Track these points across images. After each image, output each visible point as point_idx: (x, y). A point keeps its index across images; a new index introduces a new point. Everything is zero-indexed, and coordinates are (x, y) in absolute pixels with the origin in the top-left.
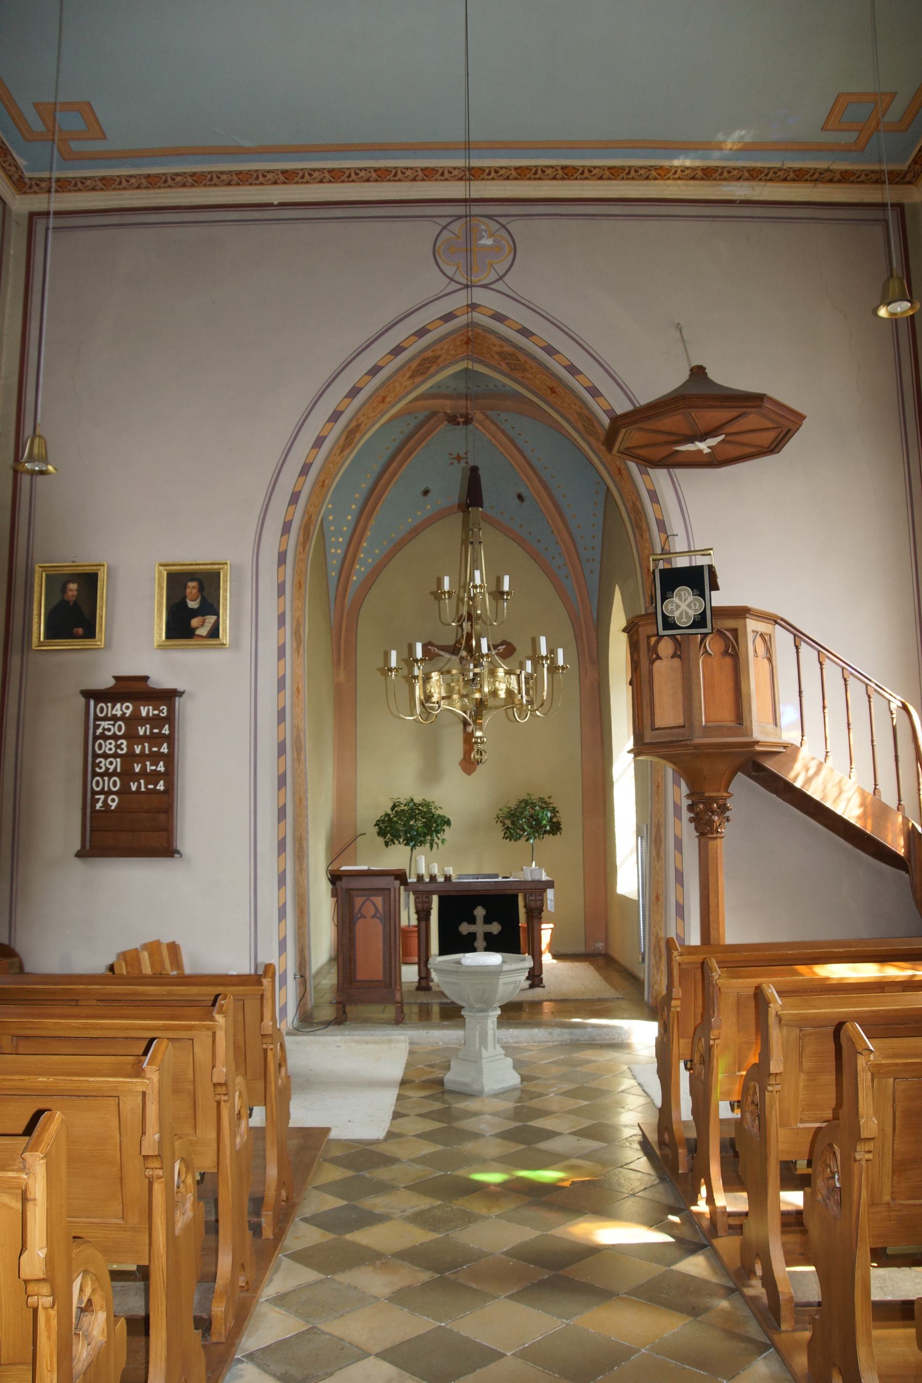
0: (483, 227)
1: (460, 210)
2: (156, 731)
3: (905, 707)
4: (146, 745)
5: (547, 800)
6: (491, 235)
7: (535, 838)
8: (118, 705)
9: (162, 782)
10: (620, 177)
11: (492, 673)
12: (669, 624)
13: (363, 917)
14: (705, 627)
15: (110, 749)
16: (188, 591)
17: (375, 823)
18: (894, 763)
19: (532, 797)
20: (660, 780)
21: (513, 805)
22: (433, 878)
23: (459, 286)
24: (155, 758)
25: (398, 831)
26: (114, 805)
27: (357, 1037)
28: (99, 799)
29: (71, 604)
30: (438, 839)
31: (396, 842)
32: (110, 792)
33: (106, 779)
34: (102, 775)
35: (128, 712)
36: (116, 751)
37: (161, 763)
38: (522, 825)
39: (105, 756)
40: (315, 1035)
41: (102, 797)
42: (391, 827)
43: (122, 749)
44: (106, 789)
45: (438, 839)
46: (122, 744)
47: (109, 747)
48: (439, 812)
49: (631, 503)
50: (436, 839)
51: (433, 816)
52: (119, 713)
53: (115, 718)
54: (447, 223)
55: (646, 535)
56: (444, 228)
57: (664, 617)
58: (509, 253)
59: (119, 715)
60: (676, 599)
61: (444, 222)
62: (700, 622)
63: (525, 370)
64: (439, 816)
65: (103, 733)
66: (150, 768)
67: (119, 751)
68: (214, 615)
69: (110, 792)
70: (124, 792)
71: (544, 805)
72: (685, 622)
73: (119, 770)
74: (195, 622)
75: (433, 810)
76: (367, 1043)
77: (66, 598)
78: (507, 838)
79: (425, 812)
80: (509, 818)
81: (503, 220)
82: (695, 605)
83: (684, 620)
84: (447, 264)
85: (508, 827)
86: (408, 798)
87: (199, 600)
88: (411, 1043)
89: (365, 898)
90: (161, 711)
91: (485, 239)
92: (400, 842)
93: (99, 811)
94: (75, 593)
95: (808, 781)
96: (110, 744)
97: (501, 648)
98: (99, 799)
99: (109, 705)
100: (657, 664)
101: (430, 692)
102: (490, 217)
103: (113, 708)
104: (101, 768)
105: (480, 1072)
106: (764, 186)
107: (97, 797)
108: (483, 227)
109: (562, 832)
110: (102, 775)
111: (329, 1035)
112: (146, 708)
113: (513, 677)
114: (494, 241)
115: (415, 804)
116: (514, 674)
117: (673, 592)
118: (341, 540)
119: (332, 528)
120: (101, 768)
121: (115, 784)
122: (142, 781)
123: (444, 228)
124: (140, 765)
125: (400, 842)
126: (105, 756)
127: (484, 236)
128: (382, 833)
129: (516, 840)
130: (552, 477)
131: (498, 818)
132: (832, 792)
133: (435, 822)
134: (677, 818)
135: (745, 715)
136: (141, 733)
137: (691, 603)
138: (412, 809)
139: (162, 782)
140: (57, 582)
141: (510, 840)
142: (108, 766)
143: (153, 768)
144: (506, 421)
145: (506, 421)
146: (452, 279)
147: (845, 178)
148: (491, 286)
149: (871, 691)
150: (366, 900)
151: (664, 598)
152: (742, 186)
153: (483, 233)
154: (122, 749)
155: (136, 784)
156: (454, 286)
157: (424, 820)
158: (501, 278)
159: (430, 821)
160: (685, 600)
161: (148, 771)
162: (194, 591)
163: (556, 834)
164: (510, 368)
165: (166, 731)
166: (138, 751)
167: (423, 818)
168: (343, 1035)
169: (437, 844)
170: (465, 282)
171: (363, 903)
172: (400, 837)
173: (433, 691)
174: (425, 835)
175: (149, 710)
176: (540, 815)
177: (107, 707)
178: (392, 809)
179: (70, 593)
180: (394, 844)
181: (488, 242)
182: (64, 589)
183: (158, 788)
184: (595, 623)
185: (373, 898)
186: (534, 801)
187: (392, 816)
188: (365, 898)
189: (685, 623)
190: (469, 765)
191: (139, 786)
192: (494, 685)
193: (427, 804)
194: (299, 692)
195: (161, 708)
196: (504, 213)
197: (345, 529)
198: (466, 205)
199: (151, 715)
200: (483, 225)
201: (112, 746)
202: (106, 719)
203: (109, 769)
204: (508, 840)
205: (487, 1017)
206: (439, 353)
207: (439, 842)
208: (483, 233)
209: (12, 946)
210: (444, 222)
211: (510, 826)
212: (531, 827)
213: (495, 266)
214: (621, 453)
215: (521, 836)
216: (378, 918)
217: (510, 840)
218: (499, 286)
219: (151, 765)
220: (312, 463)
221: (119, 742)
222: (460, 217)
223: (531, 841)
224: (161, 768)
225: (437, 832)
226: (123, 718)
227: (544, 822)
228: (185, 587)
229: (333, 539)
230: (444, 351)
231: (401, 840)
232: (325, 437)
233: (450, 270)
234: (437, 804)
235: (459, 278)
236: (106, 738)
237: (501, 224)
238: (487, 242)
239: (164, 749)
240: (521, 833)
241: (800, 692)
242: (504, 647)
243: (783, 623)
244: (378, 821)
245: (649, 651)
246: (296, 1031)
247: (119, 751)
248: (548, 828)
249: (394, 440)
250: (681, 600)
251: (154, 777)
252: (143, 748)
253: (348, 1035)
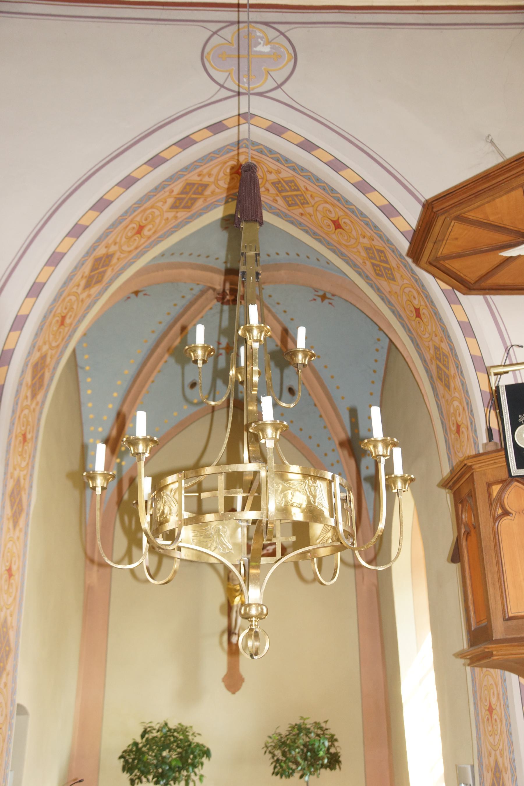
0: (258, 34)
1: (231, 15)
5: (323, 725)
6: (268, 42)
7: (311, 774)
11: (282, 475)
17: (120, 754)
19: (306, 722)
20: (494, 701)
21: (284, 731)
23: (230, 94)
25: (146, 764)
30: (196, 774)
31: (144, 779)
38: (295, 758)
42: (139, 760)
45: (196, 774)
48: (197, 740)
49: (432, 351)
50: (193, 774)
51: (190, 745)
55: (456, 383)
56: (215, 33)
58: (289, 61)
61: (215, 27)
63: (305, 203)
64: (198, 745)
71: (319, 732)
75: (190, 738)
78: (277, 774)
79: (181, 740)
80: (280, 747)
85: (278, 760)
86: (162, 722)
92: (148, 780)
100: (505, 521)
101: (163, 513)
102: (266, 24)
108: (258, 34)
109: (342, 766)
113: (321, 485)
114: (271, 48)
115: (170, 730)
116: (323, 479)
118: (100, 429)
119: (91, 416)
123: (215, 33)
125: (148, 780)
127: (260, 43)
128: (128, 768)
129: (289, 776)
130: (326, 367)
131: (267, 747)
133: (193, 753)
138: (166, 736)
141: (281, 777)
144: (278, 304)
145: (278, 304)
148: (268, 95)
153: (259, 40)
156: (225, 93)
157: (179, 750)
158: (279, 86)
159: (186, 751)
163: (335, 769)
164: (287, 202)
167: (178, 746)
169: (194, 781)
170: (236, 88)
172: (149, 773)
173: (167, 510)
174: (180, 770)
176: (317, 744)
178: (143, 736)
180: (141, 782)
186: (308, 726)
187: (140, 745)
192: (285, 496)
193: (183, 730)
194: (10, 575)
196: (284, 20)
197: (105, 418)
198: (239, 11)
200: (259, 32)
204: (279, 776)
206: (206, 180)
207: (196, 779)
208: (259, 40)
210: (215, 27)
211: (281, 758)
212: (305, 759)
214: (430, 263)
215: (294, 771)
217: (281, 777)
218: (277, 94)
220: (45, 284)
222: (232, 23)
223: (306, 778)
225: (194, 766)
227: (321, 754)
229: (92, 428)
230: (212, 179)
231: (150, 777)
232: (63, 255)
233: (220, 77)
234: (195, 729)
240: (294, 767)
244: (125, 751)
248: (326, 761)
249: (160, 323)
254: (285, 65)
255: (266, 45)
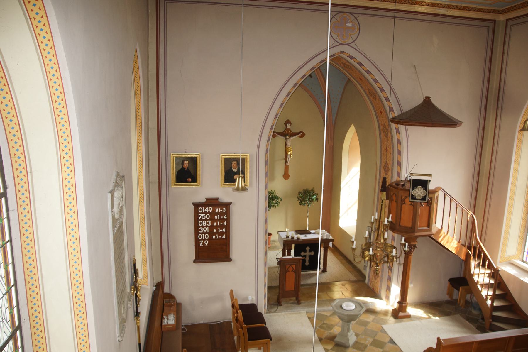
0: (348, 18)
2: (222, 217)
3: (472, 216)
4: (218, 222)
6: (351, 22)
8: (207, 208)
9: (224, 235)
10: (402, 3)
12: (413, 197)
13: (289, 271)
14: (425, 200)
15: (204, 224)
16: (233, 165)
18: (444, 200)
21: (301, 191)
22: (293, 238)
24: (222, 227)
26: (207, 244)
27: (290, 312)
28: (201, 242)
29: (186, 169)
32: (205, 239)
33: (203, 235)
34: (202, 233)
35: (211, 211)
36: (207, 225)
37: (224, 229)
39: (203, 227)
40: (276, 313)
41: (202, 241)
43: (209, 224)
44: (204, 238)
46: (209, 222)
47: (204, 223)
48: (276, 194)
52: (207, 211)
53: (206, 213)
54: (335, 14)
57: (412, 195)
58: (357, 31)
59: (207, 212)
60: (417, 190)
62: (424, 198)
65: (202, 218)
66: (220, 230)
67: (208, 225)
68: (243, 174)
69: (205, 239)
70: (210, 239)
72: (419, 198)
73: (208, 232)
74: (235, 177)
76: (293, 314)
77: (184, 167)
81: (356, 15)
82: (423, 193)
83: (419, 197)
84: (334, 34)
87: (237, 168)
88: (307, 312)
89: (289, 266)
90: (224, 210)
91: (348, 23)
93: (201, 246)
94: (188, 165)
95: (442, 240)
96: (205, 222)
97: (300, 134)
98: (201, 242)
99: (203, 208)
100: (404, 205)
102: (351, 13)
103: (205, 210)
104: (201, 231)
105: (348, 340)
106: (451, 10)
107: (200, 241)
110: (202, 233)
111: (280, 312)
112: (218, 209)
117: (416, 187)
120: (201, 231)
121: (207, 236)
122: (217, 235)
124: (216, 230)
126: (203, 227)
132: (447, 242)
134: (393, 240)
135: (430, 225)
136: (216, 218)
137: (422, 192)
139: (224, 235)
140: (180, 160)
142: (204, 230)
143: (221, 230)
146: (335, 41)
147: (480, 10)
149: (464, 211)
150: (289, 266)
151: (413, 189)
152: (444, 10)
154: (209, 224)
155: (215, 236)
158: (354, 42)
160: (420, 191)
161: (219, 231)
162: (235, 165)
165: (225, 217)
166: (215, 225)
168: (285, 312)
171: (288, 268)
175: (219, 209)
177: (203, 209)
179: (186, 165)
181: (350, 25)
182: (183, 164)
183: (223, 237)
184: (333, 124)
185: (292, 266)
188: (289, 266)
189: (419, 198)
190: (286, 176)
191: (216, 237)
195: (223, 209)
199: (219, 211)
201: (205, 223)
202: (202, 213)
203: (204, 231)
205: (350, 324)
208: (348, 21)
209: (171, 293)
213: (351, 35)
216: (293, 271)
219: (220, 230)
221: (208, 222)
222: (340, 12)
224: (224, 230)
226: (209, 213)
228: (232, 164)
235: (338, 40)
236: (203, 220)
237: (355, 17)
238: (350, 25)
239: (225, 224)
241: (443, 212)
242: (301, 134)
243: (442, 190)
245: (401, 201)
246: (269, 311)
247: (208, 225)
250: (419, 190)
251: (222, 234)
252: (217, 223)
253: (287, 312)
254: (356, 32)
255: (350, 23)
